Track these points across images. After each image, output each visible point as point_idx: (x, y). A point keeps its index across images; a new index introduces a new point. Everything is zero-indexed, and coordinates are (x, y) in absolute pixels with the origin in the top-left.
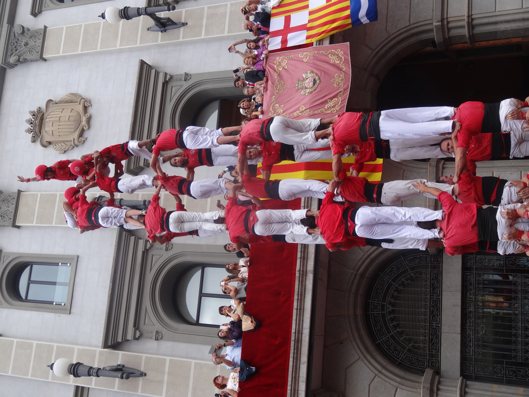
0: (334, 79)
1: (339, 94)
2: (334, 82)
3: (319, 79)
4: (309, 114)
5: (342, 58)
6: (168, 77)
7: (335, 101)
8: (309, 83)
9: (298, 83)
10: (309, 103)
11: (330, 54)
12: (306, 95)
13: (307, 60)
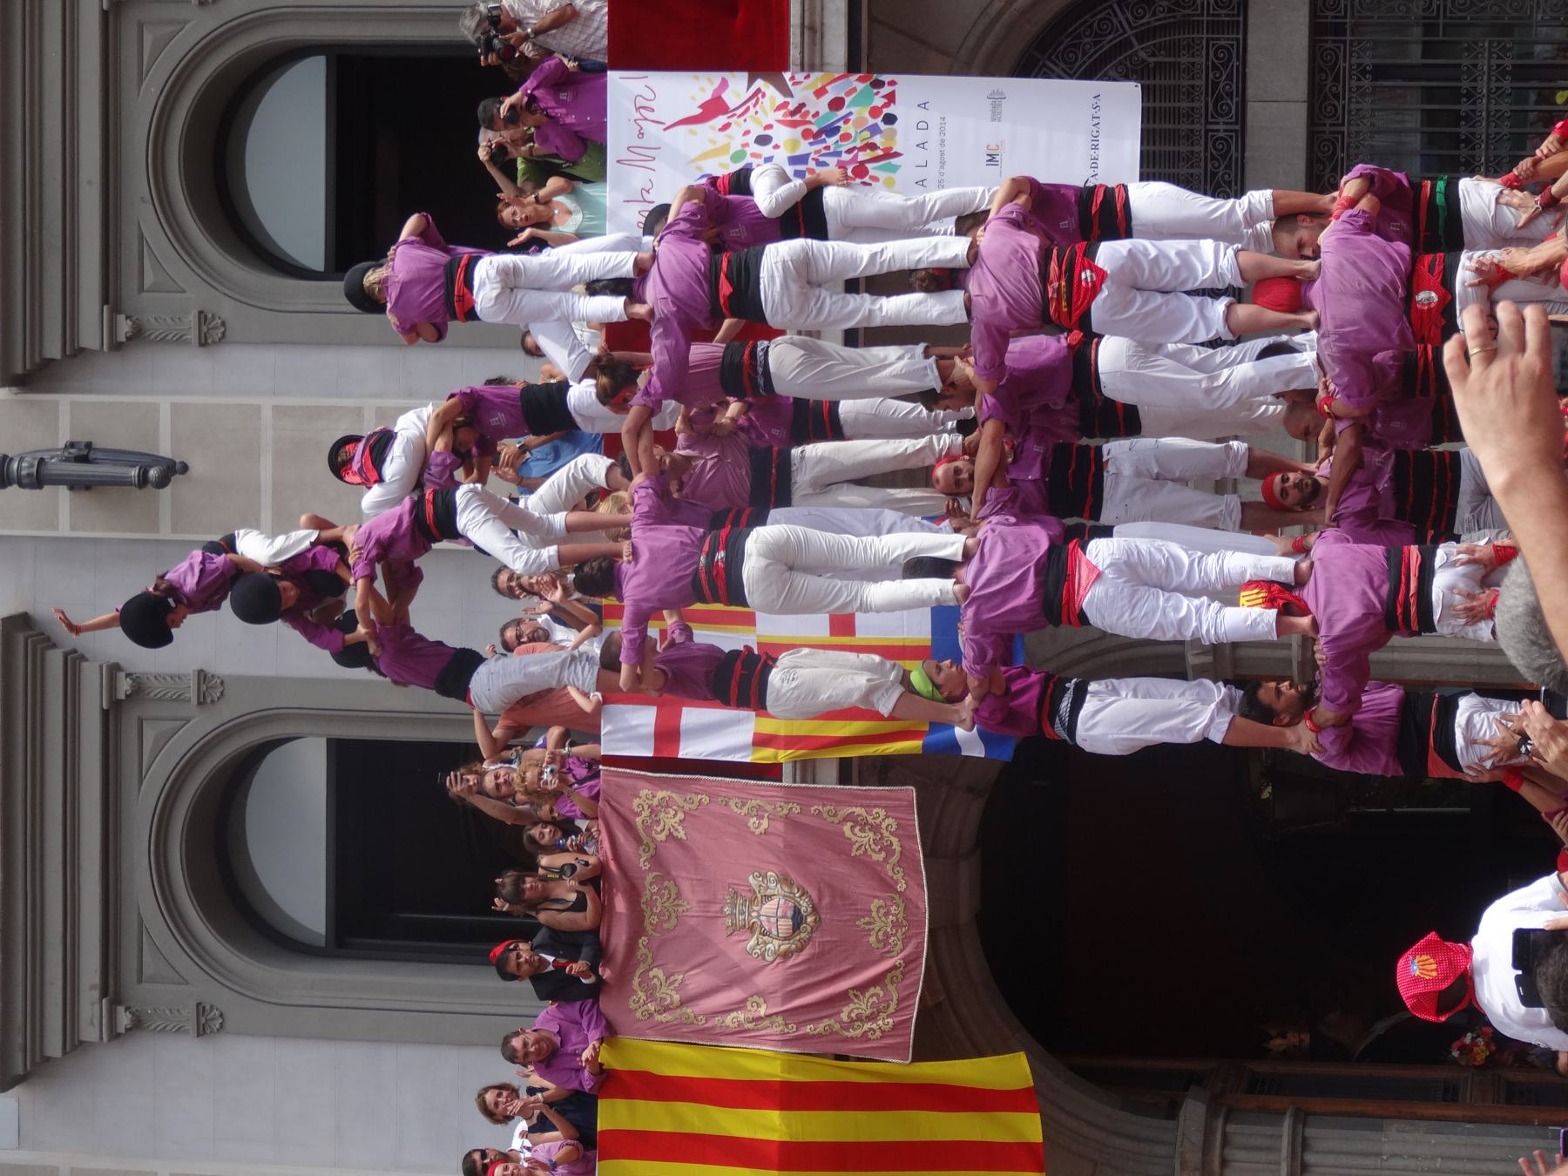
0: (867, 919)
1: (889, 975)
2: (869, 930)
3: (815, 910)
4: (783, 1033)
5: (891, 844)
6: (124, 686)
7: (875, 999)
8: (773, 910)
9: (734, 905)
10: (779, 994)
13: (762, 829)
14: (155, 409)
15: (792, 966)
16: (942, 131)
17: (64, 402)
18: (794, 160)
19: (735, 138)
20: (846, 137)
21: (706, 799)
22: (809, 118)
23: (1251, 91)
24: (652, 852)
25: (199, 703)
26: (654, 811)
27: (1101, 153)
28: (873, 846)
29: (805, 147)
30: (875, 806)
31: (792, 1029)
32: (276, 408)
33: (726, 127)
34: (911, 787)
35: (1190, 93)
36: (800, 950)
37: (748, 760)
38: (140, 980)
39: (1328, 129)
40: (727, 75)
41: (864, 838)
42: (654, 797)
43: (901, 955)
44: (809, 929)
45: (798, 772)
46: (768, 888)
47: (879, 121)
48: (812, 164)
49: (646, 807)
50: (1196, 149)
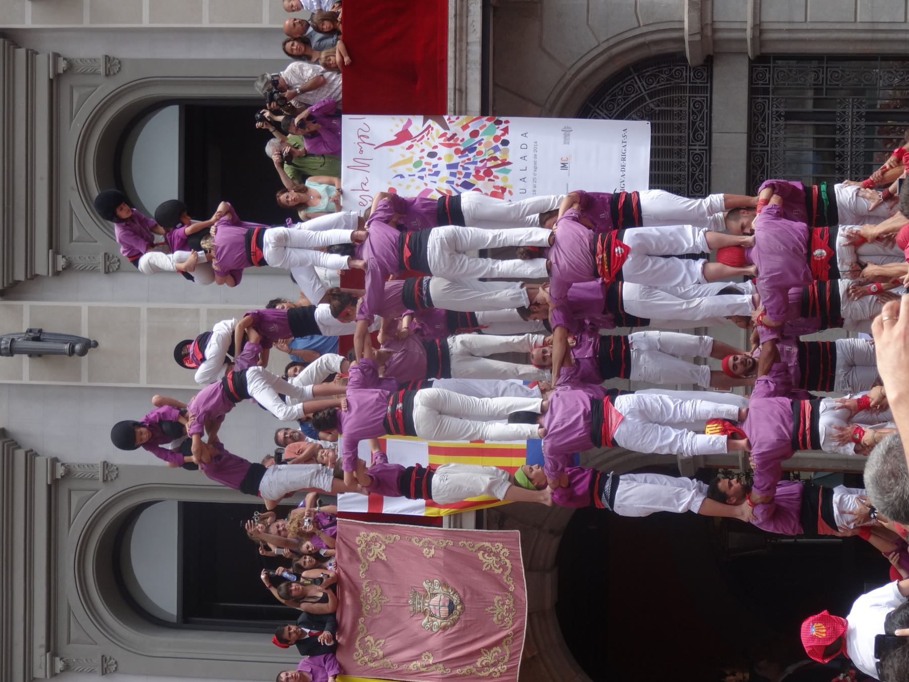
0: (492, 607)
1: (505, 641)
2: (493, 614)
3: (461, 602)
4: (443, 674)
5: (506, 564)
6: (60, 471)
7: (496, 654)
8: (437, 602)
11: (482, 552)
12: (435, 630)
13: (431, 555)
14: (79, 309)
15: (446, 636)
16: (535, 150)
17: (26, 306)
18: (450, 167)
19: (416, 154)
20: (480, 153)
21: (398, 537)
22: (459, 142)
23: (714, 127)
24: (367, 568)
25: (105, 481)
26: (368, 544)
27: (627, 162)
28: (495, 565)
29: (456, 159)
30: (497, 542)
31: (448, 671)
32: (149, 309)
33: (410, 147)
34: (518, 531)
35: (679, 128)
36: (453, 625)
37: (423, 514)
38: (69, 642)
39: (759, 149)
40: (411, 117)
41: (489, 560)
42: (368, 536)
43: (512, 629)
44: (458, 613)
45: (452, 522)
46: (434, 589)
47: (499, 144)
48: (460, 169)
49: (363, 542)
50: (683, 160)
